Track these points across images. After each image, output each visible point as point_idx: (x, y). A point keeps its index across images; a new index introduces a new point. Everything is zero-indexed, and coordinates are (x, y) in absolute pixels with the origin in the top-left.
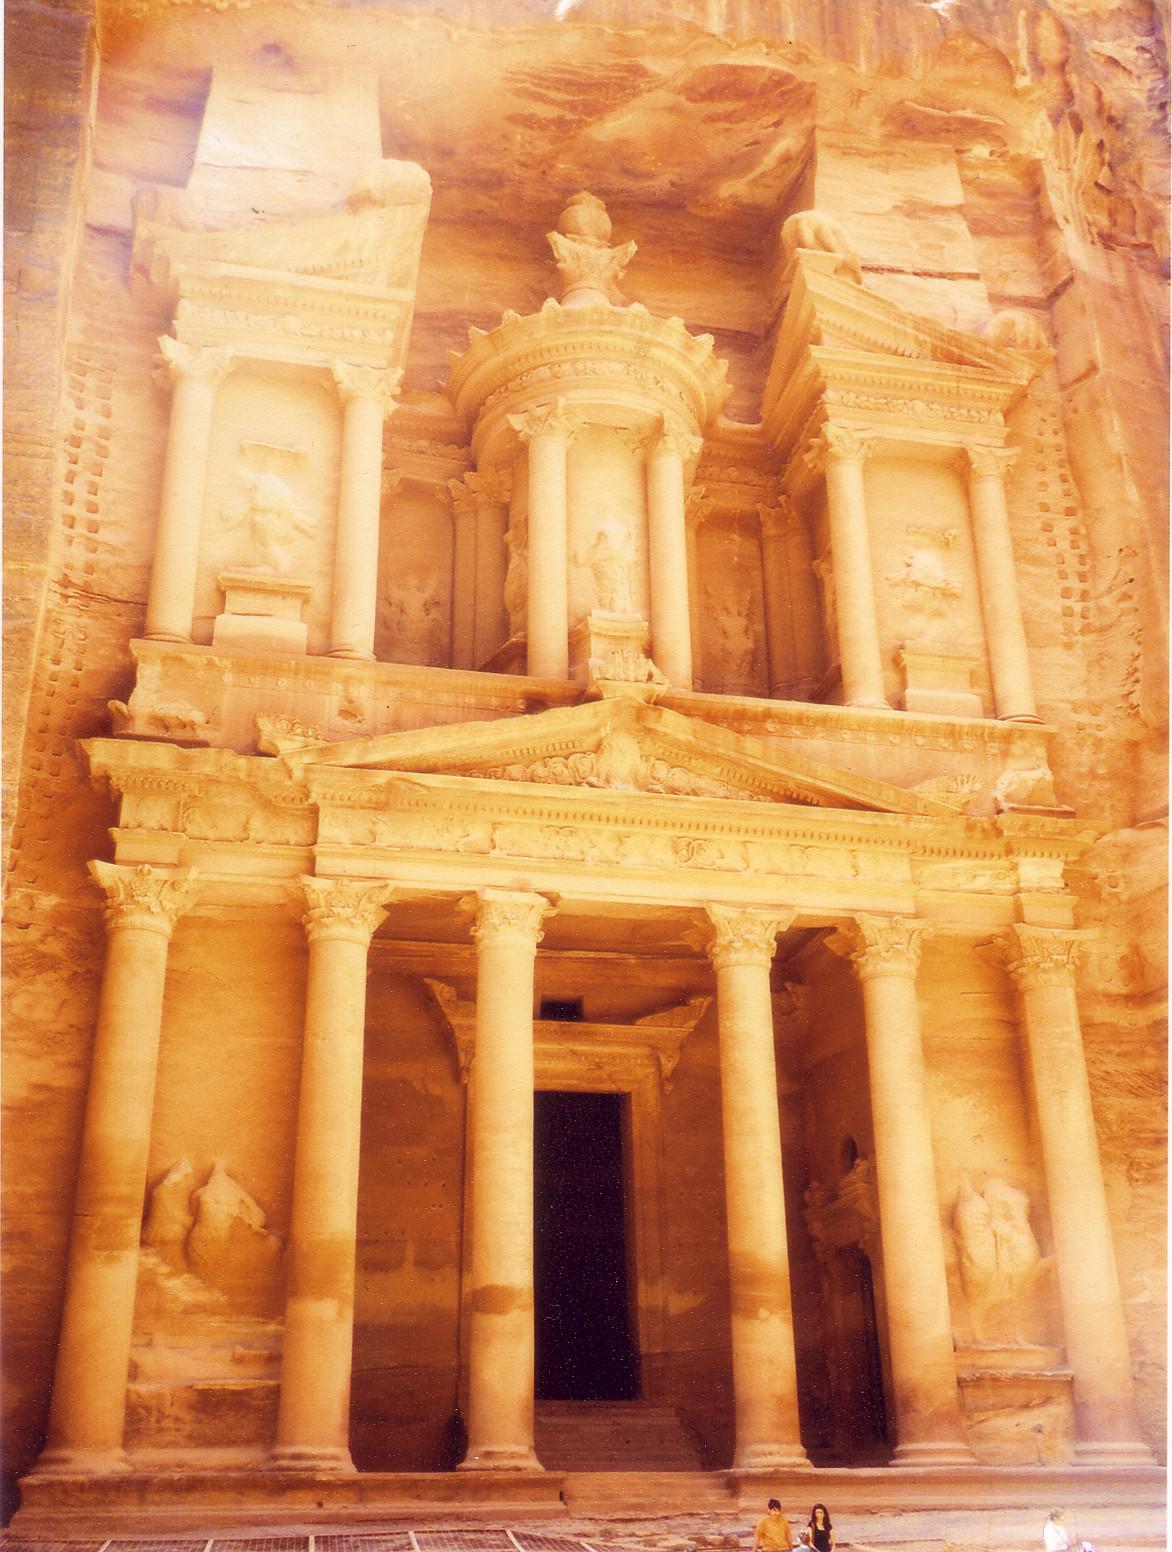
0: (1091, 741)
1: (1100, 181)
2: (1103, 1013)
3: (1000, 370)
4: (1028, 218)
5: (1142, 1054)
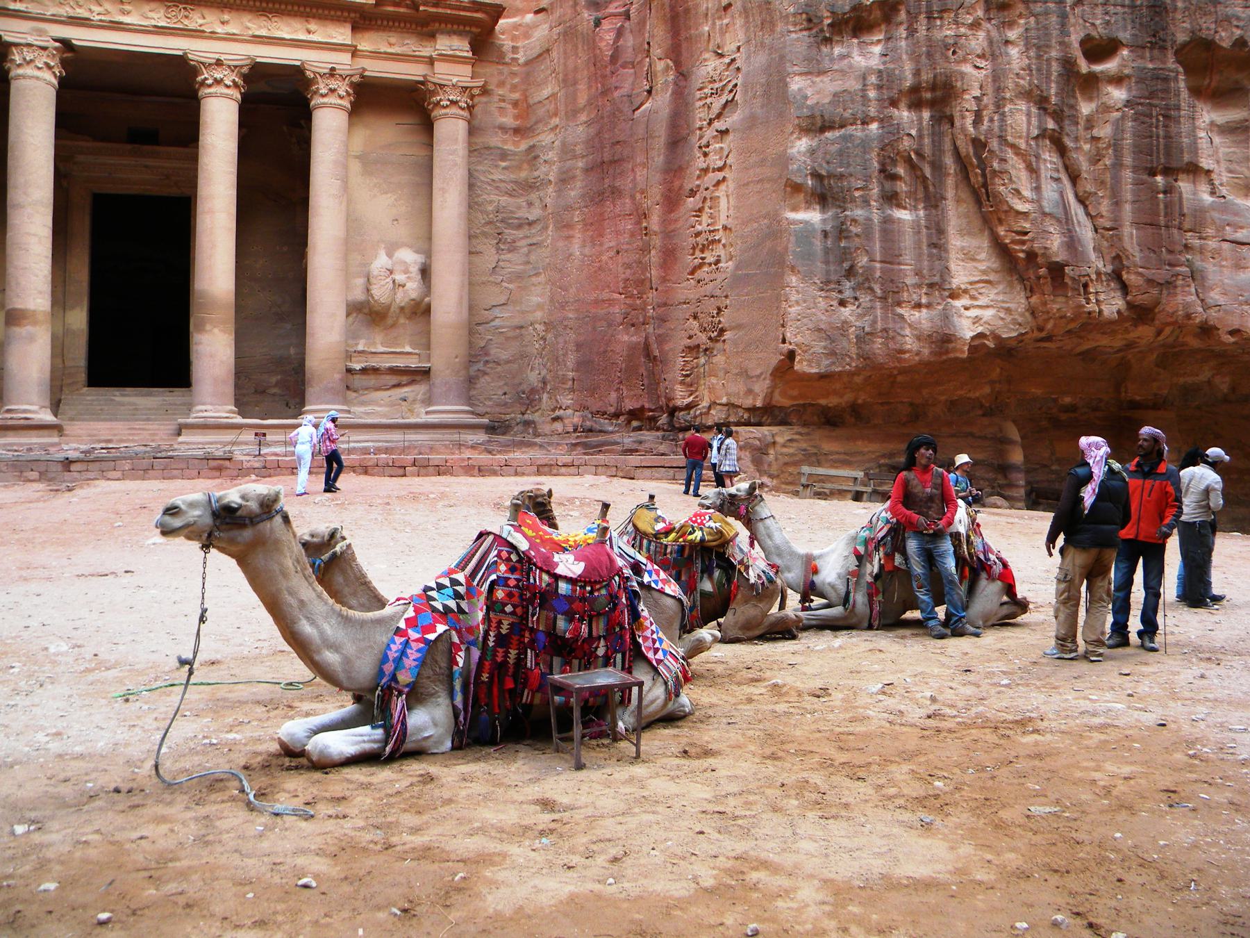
2: (496, 140)
5: (519, 168)
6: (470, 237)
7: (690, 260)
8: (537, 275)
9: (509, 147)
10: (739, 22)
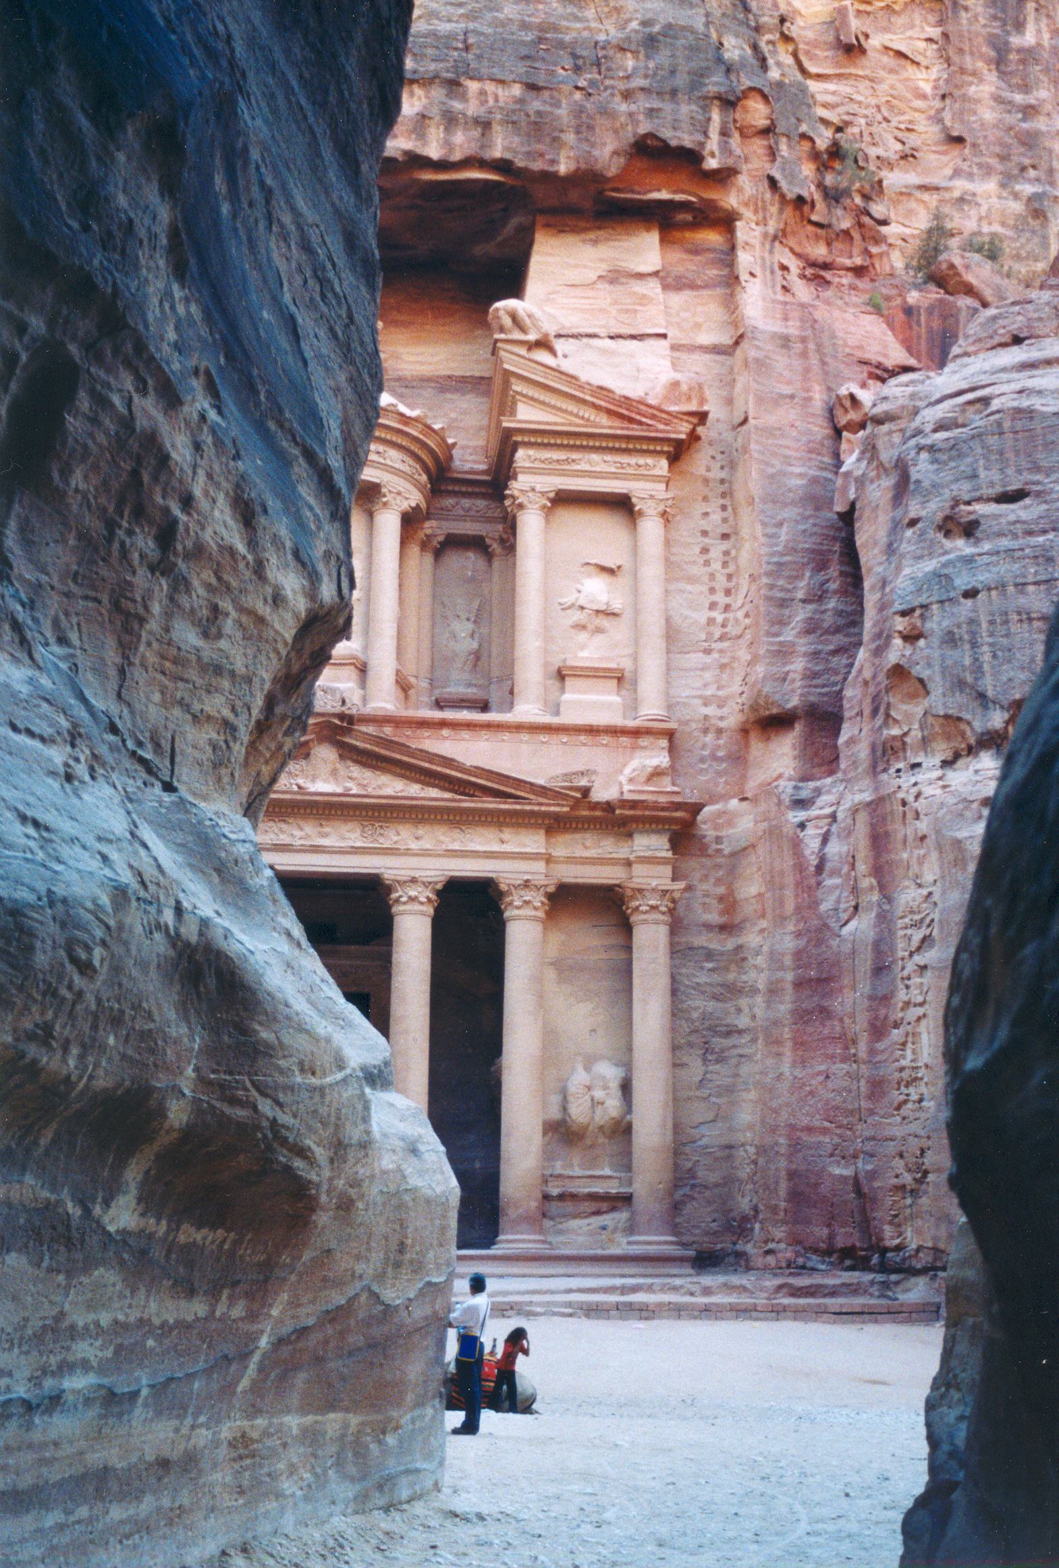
0: (713, 730)
1: (814, 218)
2: (701, 940)
3: (661, 427)
4: (726, 271)
5: (727, 969)
6: (675, 1048)
7: (896, 1096)
8: (748, 1090)
9: (714, 946)
10: (934, 856)
